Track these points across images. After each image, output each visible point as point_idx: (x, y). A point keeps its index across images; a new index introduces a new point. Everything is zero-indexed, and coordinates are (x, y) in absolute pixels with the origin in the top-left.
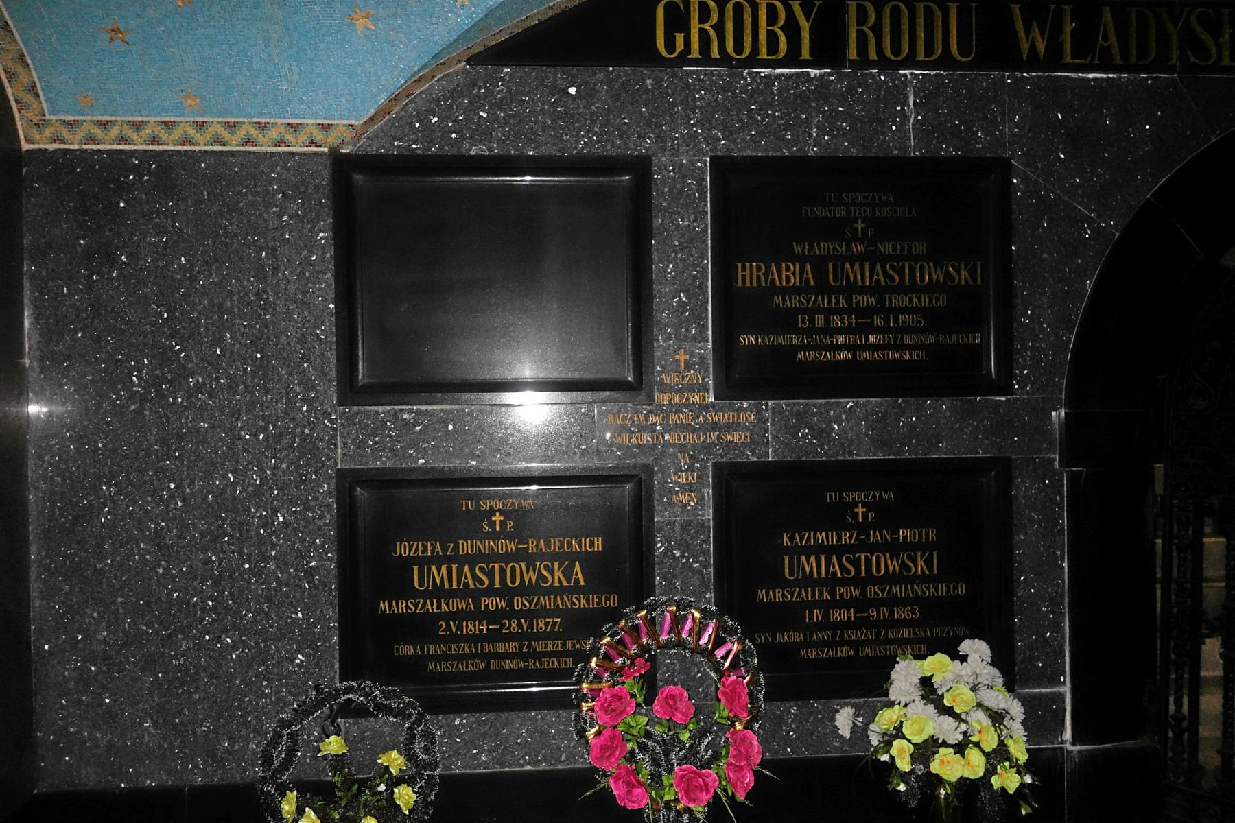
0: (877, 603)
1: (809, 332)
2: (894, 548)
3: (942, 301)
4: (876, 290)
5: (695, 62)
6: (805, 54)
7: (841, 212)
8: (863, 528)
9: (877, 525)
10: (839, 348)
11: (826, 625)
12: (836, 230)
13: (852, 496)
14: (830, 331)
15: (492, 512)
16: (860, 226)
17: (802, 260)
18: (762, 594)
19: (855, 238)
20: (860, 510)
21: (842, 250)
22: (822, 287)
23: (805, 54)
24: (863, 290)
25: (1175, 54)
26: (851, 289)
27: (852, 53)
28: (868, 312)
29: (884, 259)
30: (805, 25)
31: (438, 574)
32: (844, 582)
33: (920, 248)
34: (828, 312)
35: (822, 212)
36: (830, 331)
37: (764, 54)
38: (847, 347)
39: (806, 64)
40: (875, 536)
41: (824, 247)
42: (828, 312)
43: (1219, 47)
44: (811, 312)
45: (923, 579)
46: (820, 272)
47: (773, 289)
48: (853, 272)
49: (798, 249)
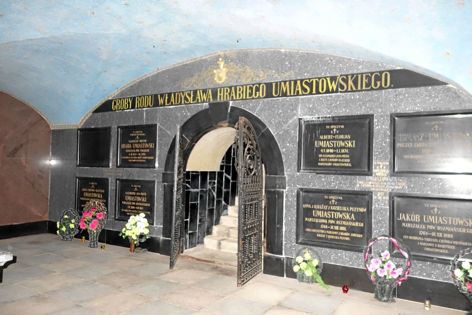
0: (137, 206)
1: (130, 156)
2: (140, 196)
3: (148, 151)
4: (139, 149)
5: (117, 110)
6: (130, 107)
7: (135, 135)
8: (136, 192)
9: (138, 192)
10: (133, 159)
11: (130, 209)
12: (134, 138)
13: (135, 186)
14: (133, 156)
15: (92, 185)
16: (137, 137)
17: (130, 143)
18: (123, 202)
19: (137, 140)
20: (136, 189)
21: (135, 141)
22: (132, 148)
23: (130, 107)
24: (138, 149)
25: (183, 101)
26: (136, 149)
27: (136, 107)
28: (137, 153)
29: (141, 143)
30: (130, 102)
31: (86, 194)
32: (133, 202)
33: (145, 141)
34: (133, 153)
35: (132, 135)
36: (133, 156)
37: (125, 108)
38: (136, 159)
39: (130, 109)
40: (138, 194)
41: (133, 141)
42: (133, 153)
43: (190, 99)
44: (130, 153)
45: (144, 202)
46: (132, 146)
47: (126, 149)
48: (136, 146)
49: (130, 141)
